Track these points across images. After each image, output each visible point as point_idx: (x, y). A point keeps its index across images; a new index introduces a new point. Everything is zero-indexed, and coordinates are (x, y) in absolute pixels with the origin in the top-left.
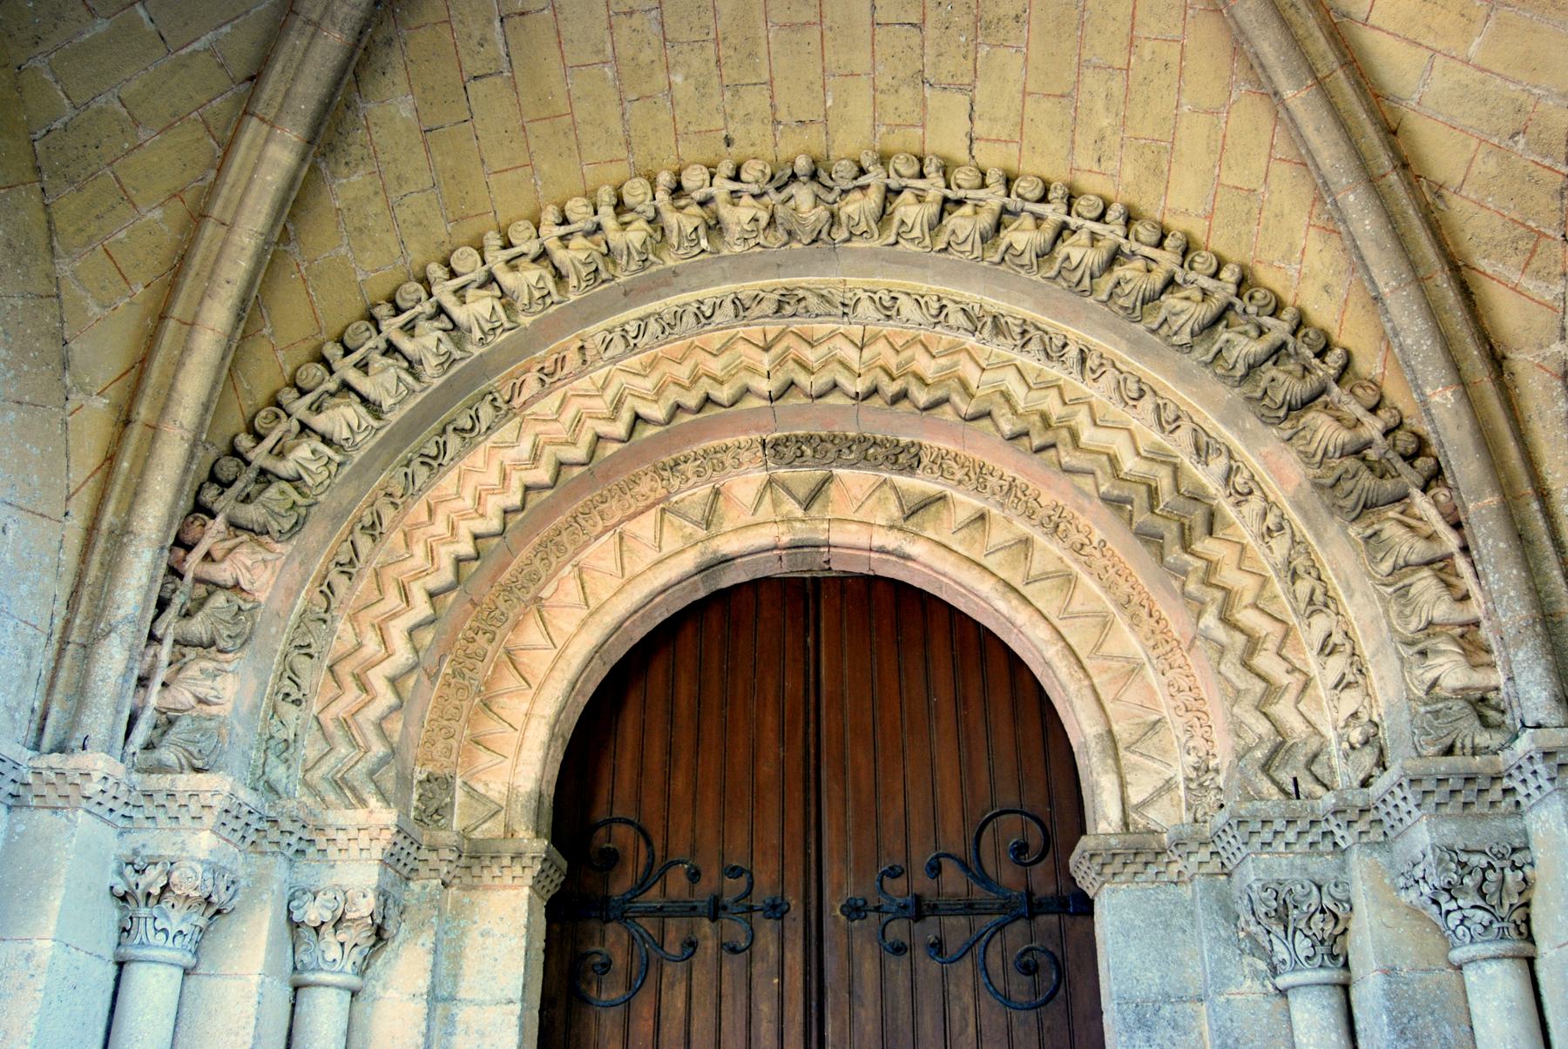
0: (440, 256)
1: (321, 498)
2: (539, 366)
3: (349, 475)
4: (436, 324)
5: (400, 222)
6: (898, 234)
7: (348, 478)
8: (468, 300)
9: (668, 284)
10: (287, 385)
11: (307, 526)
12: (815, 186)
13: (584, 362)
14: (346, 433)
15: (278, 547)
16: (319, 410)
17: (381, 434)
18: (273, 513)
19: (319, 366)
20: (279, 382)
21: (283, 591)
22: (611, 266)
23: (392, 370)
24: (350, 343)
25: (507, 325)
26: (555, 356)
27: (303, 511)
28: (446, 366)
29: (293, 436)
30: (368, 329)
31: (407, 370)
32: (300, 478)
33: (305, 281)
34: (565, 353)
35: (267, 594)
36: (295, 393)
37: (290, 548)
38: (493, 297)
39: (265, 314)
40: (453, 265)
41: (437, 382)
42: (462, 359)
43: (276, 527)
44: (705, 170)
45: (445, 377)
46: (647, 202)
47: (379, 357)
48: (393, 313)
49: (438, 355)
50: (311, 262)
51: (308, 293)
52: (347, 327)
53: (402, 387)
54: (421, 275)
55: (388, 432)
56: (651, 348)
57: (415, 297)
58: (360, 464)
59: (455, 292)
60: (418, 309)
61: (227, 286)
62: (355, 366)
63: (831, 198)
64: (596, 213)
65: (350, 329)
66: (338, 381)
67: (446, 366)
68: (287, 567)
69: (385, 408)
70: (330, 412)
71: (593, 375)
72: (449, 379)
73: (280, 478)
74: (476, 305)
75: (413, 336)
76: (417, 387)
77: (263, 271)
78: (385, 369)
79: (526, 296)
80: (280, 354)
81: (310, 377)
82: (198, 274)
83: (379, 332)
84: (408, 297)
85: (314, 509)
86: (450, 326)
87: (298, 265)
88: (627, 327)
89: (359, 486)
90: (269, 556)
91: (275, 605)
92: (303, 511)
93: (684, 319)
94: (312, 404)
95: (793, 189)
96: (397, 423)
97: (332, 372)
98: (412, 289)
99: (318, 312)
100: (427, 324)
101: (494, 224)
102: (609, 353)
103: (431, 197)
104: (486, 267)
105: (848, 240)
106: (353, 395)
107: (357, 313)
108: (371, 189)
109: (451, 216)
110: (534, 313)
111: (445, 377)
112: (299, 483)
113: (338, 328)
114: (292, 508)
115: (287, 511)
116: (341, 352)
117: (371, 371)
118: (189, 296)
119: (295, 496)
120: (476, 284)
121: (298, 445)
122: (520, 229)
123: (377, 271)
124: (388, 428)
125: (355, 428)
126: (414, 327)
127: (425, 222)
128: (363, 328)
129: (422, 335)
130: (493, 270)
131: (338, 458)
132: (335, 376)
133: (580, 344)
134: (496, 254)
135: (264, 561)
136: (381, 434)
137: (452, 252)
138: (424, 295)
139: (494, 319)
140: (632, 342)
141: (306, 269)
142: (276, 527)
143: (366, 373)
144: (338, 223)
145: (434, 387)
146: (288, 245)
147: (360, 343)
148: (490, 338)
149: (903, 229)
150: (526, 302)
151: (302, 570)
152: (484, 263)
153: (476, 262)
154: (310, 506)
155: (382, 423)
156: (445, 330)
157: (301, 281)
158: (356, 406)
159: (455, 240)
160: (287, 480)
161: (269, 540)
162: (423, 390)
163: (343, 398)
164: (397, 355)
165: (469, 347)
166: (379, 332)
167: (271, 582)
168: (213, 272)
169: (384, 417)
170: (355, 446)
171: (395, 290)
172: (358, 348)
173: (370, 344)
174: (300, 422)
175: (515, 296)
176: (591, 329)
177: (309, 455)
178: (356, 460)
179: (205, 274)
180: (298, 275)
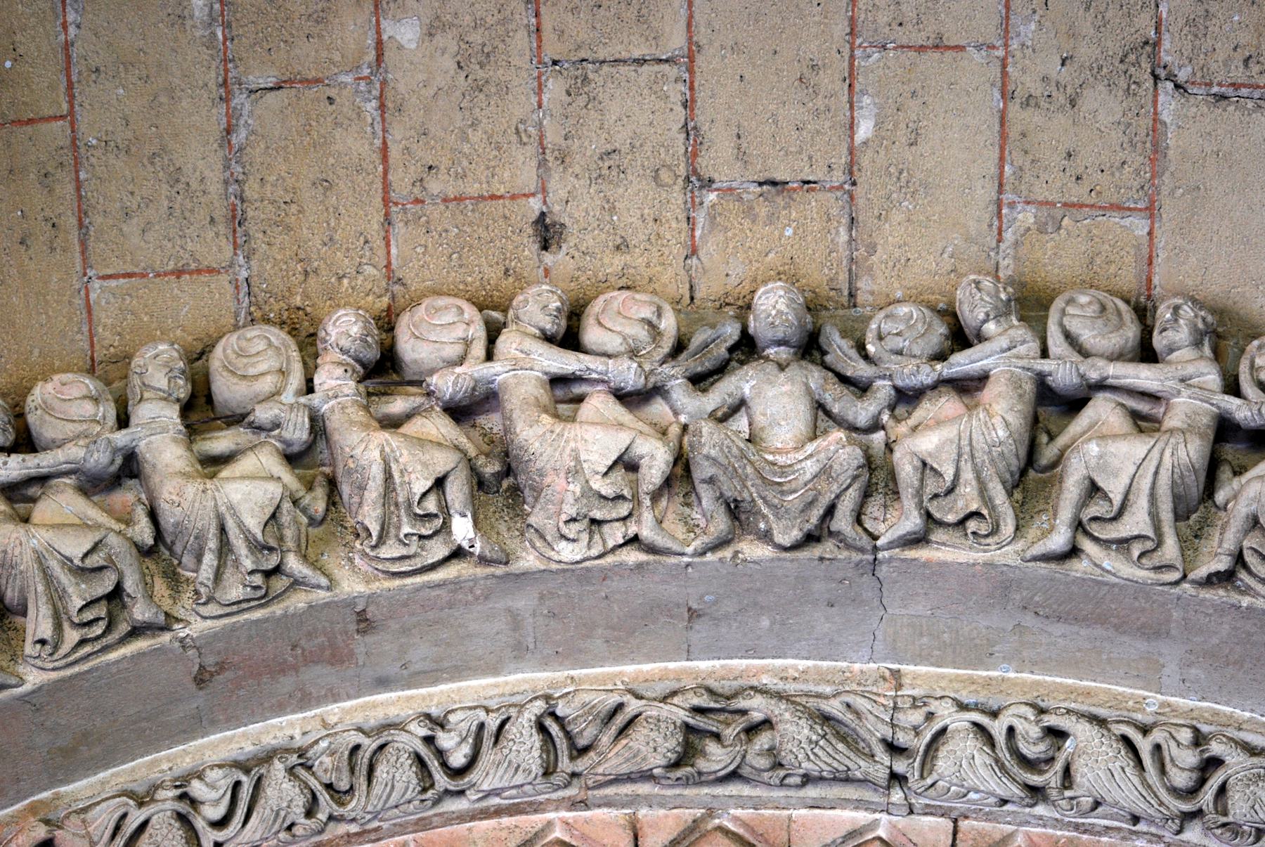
6: (1079, 526)
12: (815, 377)
44: (470, 312)
63: (862, 412)
95: (744, 382)
105: (918, 540)
149: (1097, 509)
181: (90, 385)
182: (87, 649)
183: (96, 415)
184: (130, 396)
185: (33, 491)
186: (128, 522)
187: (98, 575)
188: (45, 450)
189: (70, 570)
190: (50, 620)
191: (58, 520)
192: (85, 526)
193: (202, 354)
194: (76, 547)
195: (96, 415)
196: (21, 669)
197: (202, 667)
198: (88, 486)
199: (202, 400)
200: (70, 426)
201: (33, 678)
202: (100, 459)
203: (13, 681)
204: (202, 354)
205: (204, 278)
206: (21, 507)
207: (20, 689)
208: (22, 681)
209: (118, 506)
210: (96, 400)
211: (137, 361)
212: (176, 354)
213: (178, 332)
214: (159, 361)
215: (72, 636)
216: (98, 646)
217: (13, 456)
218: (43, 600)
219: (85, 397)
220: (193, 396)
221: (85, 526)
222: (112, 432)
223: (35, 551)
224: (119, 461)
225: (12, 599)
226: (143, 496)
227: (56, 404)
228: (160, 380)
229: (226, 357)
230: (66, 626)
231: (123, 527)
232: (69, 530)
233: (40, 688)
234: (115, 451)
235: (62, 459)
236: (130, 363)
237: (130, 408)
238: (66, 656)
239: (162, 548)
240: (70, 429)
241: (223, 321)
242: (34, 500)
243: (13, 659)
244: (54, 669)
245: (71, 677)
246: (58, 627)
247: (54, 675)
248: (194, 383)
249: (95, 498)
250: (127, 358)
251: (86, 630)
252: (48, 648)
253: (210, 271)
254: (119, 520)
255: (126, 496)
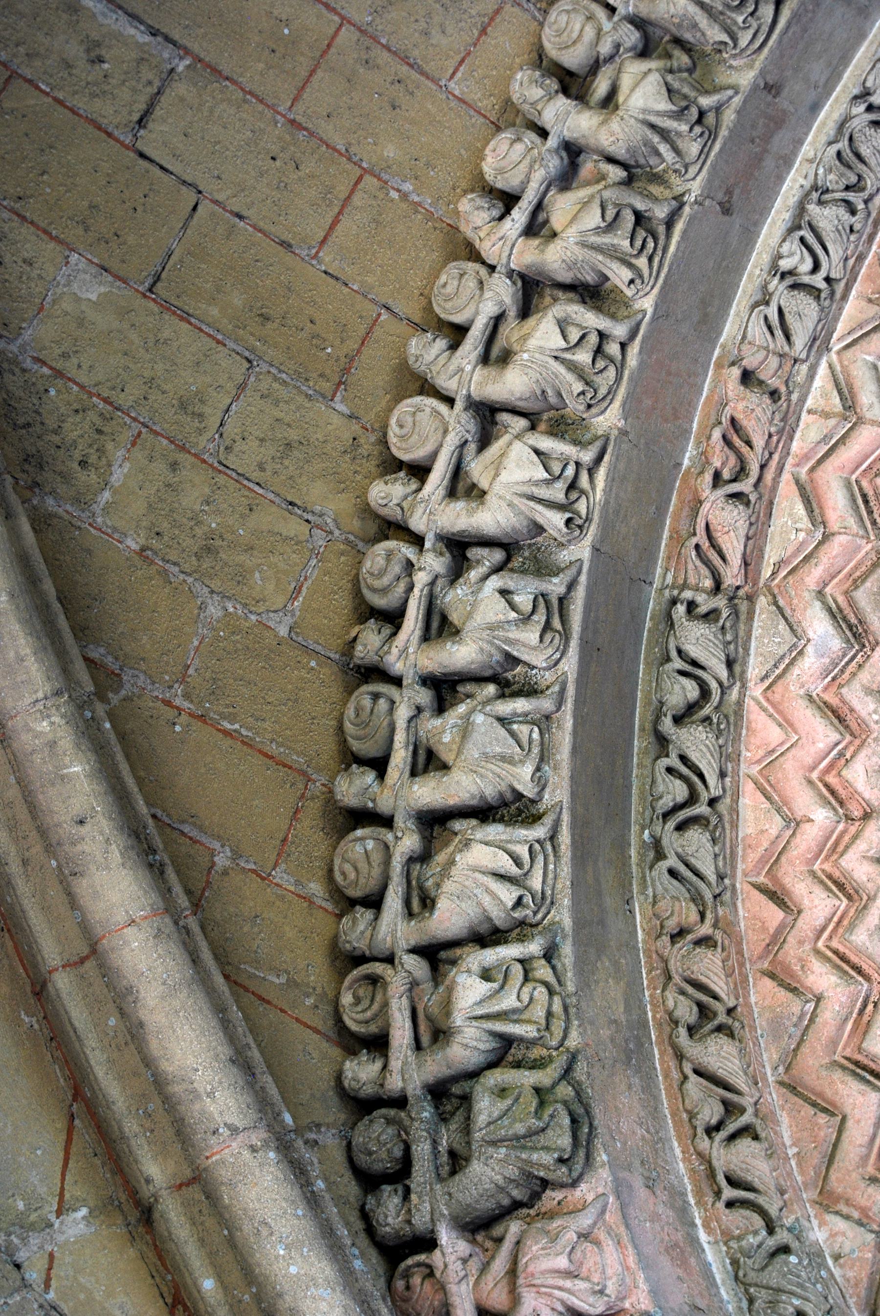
0: (371, 466)
1: (574, 1041)
2: (708, 477)
3: (581, 962)
4: (474, 575)
5: (256, 475)
7: (582, 964)
8: (484, 484)
9: (778, 121)
10: (340, 916)
11: (597, 1111)
13: (774, 395)
14: (508, 894)
15: (585, 1191)
16: (428, 902)
17: (565, 837)
18: (519, 1141)
19: (359, 832)
20: (323, 924)
21: (665, 1262)
22: (656, 190)
23: (479, 718)
24: (368, 748)
25: (587, 456)
26: (717, 434)
27: (565, 1091)
28: (557, 623)
29: (428, 986)
30: (376, 696)
31: (502, 696)
32: (507, 1042)
33: (202, 718)
34: (728, 412)
35: (643, 1286)
36: (364, 915)
37: (604, 1174)
38: (518, 437)
39: (194, 833)
40: (405, 457)
41: (570, 665)
42: (571, 586)
43: (548, 1158)
45: (574, 643)
46: (607, 26)
47: (437, 722)
48: (387, 631)
49: (526, 619)
50: (183, 679)
51: (226, 733)
52: (340, 729)
53: (523, 730)
54: (372, 528)
55: (573, 826)
56: (861, 258)
57: (396, 568)
58: (579, 924)
59: (452, 493)
60: (421, 579)
61: (84, 830)
62: (414, 773)
64: (543, 134)
65: (348, 726)
66: (410, 824)
67: (557, 623)
68: (632, 1212)
69: (528, 790)
70: (449, 886)
71: (809, 403)
72: (581, 639)
73: (474, 1075)
74: (504, 477)
75: (458, 632)
76: (546, 704)
77: (120, 757)
78: (465, 730)
79: (570, 377)
80: (280, 876)
81: (363, 866)
82: (25, 862)
83: (397, 681)
84: (386, 581)
85: (581, 1071)
86: (498, 556)
87: (168, 703)
88: (785, 264)
89: (616, 964)
90: (585, 1221)
91: (678, 1297)
92: (565, 1091)
93: (865, 151)
94: (407, 903)
96: (574, 795)
97: (387, 822)
98: (381, 561)
99: (273, 749)
100: (460, 591)
101: (403, 328)
102: (800, 340)
103: (264, 386)
104: (459, 405)
106: (458, 825)
107: (334, 691)
108: (160, 467)
109: (326, 386)
110: (611, 392)
111: (574, 643)
112: (515, 1053)
113: (329, 747)
114: (542, 1104)
115: (538, 1113)
116: (370, 777)
117: (447, 757)
118: (45, 909)
119: (528, 1078)
120: (472, 447)
121: (450, 990)
122: (449, 289)
123: (298, 590)
124: (566, 817)
125: (514, 870)
126: (444, 619)
127: (293, 435)
128: (367, 702)
129: (469, 616)
130: (476, 395)
131: (534, 947)
132: (399, 822)
133: (736, 372)
134: (452, 367)
135: (584, 1236)
136: (565, 837)
137: (384, 442)
138: (408, 551)
139: (556, 468)
140: (818, 281)
141: (187, 696)
142: (548, 1158)
143: (445, 767)
144: (164, 574)
145: (572, 678)
146: (121, 685)
147: (383, 732)
148: (582, 507)
150: (578, 387)
151: (664, 1196)
152: (450, 401)
153: (436, 412)
154: (567, 1072)
155: (548, 820)
156: (497, 569)
157: (197, 725)
158: (479, 835)
159: (370, 418)
160: (492, 1065)
161: (558, 1195)
162: (560, 702)
163: (447, 844)
164: (460, 689)
165: (565, 556)
166: (397, 681)
167: (631, 1261)
168: (43, 832)
169: (542, 807)
170: (544, 901)
171: (357, 593)
172: (391, 741)
173: (403, 713)
174: (414, 951)
175: (553, 400)
176: (729, 330)
177: (484, 988)
178: (567, 922)
179: (37, 849)
180: (184, 718)
181: (507, 135)
182: (656, 260)
183: (527, 146)
184: (532, 118)
185: (541, 217)
186: (603, 177)
187: (619, 219)
188: (523, 191)
189: (604, 232)
190: (623, 267)
191: (569, 217)
192: (585, 204)
193: (540, 56)
194: (593, 219)
195: (527, 146)
196: (637, 306)
197: (720, 204)
198: (564, 184)
199: (567, 78)
200: (521, 166)
201: (647, 304)
202: (554, 164)
203: (640, 316)
204: (540, 56)
205: (498, 19)
206: (544, 232)
207: (648, 317)
208: (644, 312)
209: (589, 176)
210: (519, 139)
211: (515, 98)
212: (529, 72)
213: (517, 60)
214: (525, 84)
215: (642, 262)
216: (659, 252)
217: (513, 212)
218: (608, 262)
219: (511, 144)
220: (561, 82)
221: (585, 204)
222: (544, 145)
223: (577, 244)
224: (564, 154)
225: (593, 279)
226: (595, 157)
227: (503, 164)
228: (537, 93)
229: (554, 44)
230: (633, 261)
231: (603, 183)
232: (580, 214)
233: (656, 305)
234: (557, 151)
235: (537, 186)
236: (513, 103)
237: (539, 123)
238: (650, 275)
239: (634, 170)
240: (523, 167)
241: (532, 28)
242: (547, 221)
243: (627, 306)
244: (652, 288)
245: (665, 282)
246: (630, 266)
247: (656, 291)
248: (553, 74)
249: (574, 185)
250: (508, 103)
251: (645, 252)
252: (638, 281)
253: (497, 12)
254: (598, 182)
255: (587, 168)
